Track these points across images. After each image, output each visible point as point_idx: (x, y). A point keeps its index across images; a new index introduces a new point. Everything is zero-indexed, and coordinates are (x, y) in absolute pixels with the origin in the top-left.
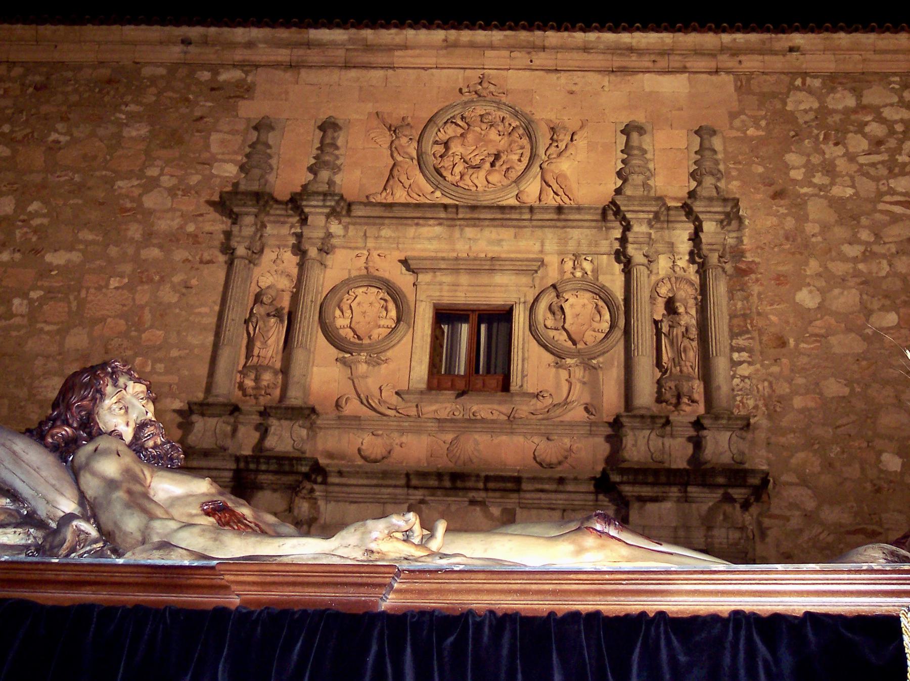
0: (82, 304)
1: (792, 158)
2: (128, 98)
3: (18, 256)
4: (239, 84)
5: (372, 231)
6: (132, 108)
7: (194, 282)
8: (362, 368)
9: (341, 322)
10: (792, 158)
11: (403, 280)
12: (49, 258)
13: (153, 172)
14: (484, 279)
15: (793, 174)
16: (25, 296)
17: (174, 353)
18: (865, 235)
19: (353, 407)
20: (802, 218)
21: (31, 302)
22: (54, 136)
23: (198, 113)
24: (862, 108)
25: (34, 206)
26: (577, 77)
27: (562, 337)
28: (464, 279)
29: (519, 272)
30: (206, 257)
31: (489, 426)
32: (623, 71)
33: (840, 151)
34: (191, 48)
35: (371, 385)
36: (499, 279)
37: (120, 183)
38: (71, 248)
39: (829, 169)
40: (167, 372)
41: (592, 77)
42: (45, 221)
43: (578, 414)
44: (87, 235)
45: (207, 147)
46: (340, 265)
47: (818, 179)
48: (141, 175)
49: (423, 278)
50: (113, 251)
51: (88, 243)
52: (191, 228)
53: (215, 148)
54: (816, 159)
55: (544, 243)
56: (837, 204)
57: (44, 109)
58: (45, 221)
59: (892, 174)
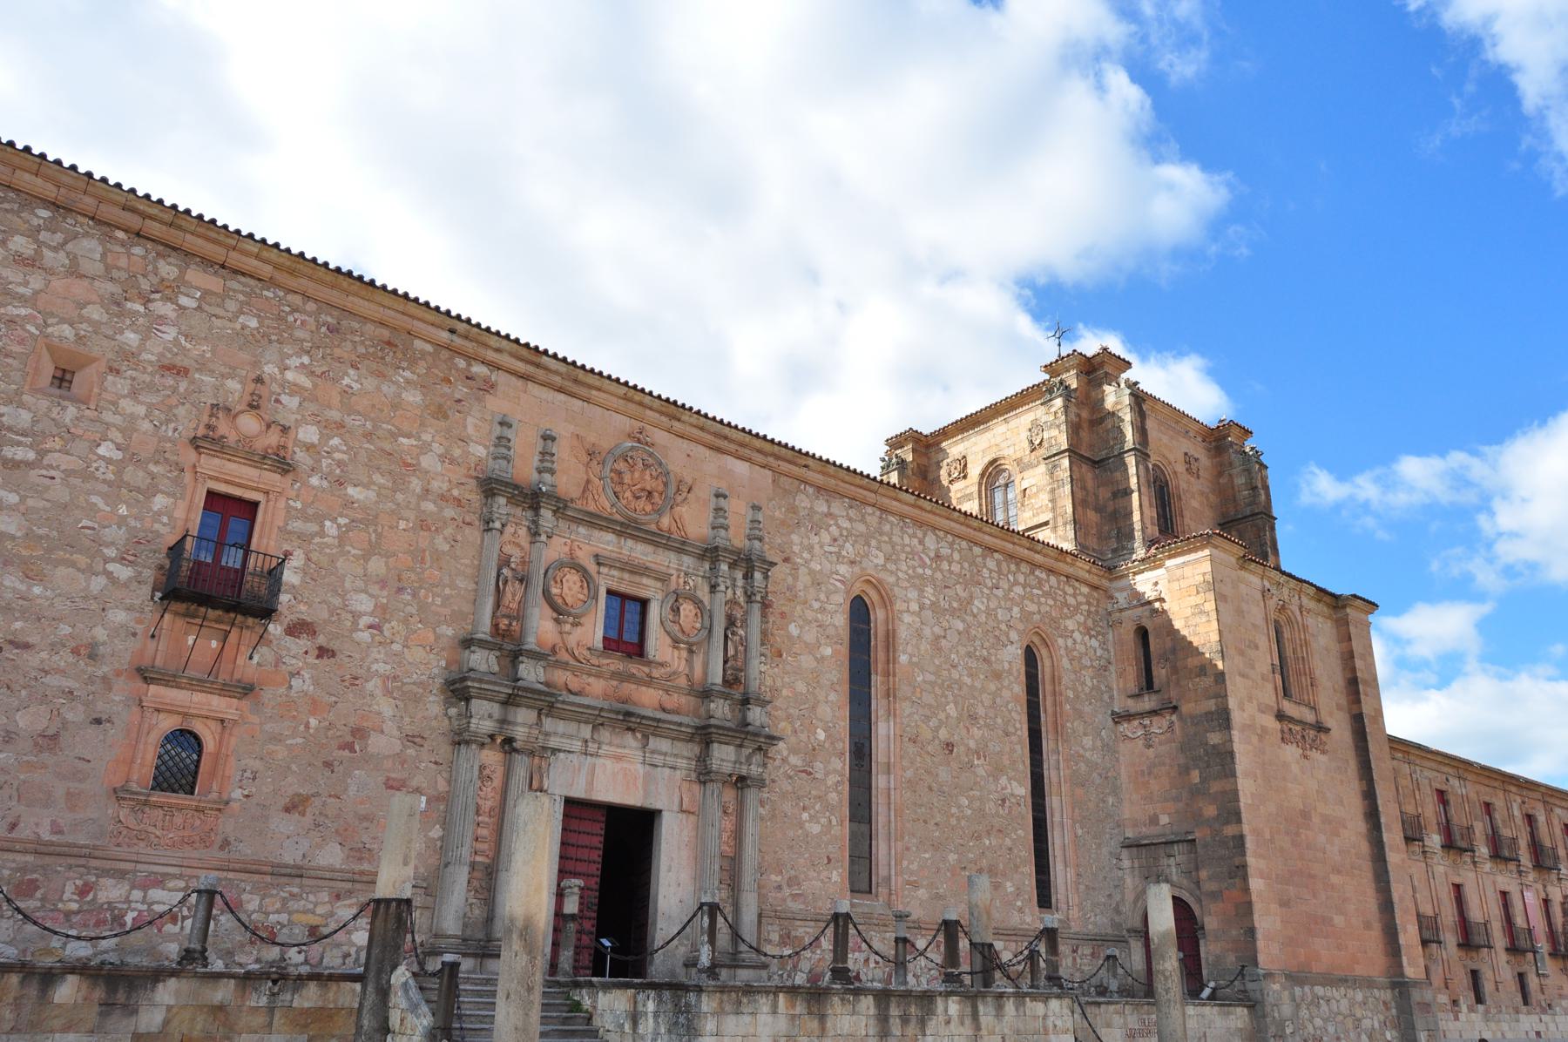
0: (379, 536)
1: (795, 537)
2: (404, 364)
3: (325, 484)
4: (486, 380)
5: (574, 526)
6: (407, 374)
7: (459, 538)
8: (568, 627)
9: (555, 591)
10: (795, 537)
11: (592, 567)
12: (351, 491)
13: (427, 437)
14: (637, 579)
15: (796, 549)
16: (334, 520)
17: (447, 591)
18: (822, 596)
19: (564, 656)
20: (796, 578)
21: (339, 526)
22: (346, 381)
23: (457, 396)
24: (829, 515)
25: (336, 441)
26: (693, 446)
27: (676, 628)
28: (626, 576)
29: (656, 579)
30: (468, 519)
31: (640, 682)
32: (719, 450)
33: (816, 539)
34: (454, 337)
35: (572, 641)
36: (645, 581)
37: (401, 439)
38: (367, 486)
39: (810, 549)
40: (443, 605)
41: (701, 449)
42: (345, 457)
43: (683, 682)
44: (377, 478)
45: (465, 427)
46: (555, 550)
47: (806, 555)
48: (419, 438)
49: (604, 570)
50: (400, 497)
51: (381, 487)
52: (455, 492)
53: (470, 430)
54: (806, 542)
55: (665, 560)
56: (811, 572)
57: (337, 352)
58: (345, 457)
59: (838, 562)
